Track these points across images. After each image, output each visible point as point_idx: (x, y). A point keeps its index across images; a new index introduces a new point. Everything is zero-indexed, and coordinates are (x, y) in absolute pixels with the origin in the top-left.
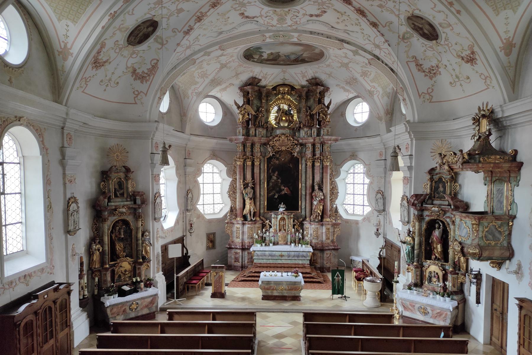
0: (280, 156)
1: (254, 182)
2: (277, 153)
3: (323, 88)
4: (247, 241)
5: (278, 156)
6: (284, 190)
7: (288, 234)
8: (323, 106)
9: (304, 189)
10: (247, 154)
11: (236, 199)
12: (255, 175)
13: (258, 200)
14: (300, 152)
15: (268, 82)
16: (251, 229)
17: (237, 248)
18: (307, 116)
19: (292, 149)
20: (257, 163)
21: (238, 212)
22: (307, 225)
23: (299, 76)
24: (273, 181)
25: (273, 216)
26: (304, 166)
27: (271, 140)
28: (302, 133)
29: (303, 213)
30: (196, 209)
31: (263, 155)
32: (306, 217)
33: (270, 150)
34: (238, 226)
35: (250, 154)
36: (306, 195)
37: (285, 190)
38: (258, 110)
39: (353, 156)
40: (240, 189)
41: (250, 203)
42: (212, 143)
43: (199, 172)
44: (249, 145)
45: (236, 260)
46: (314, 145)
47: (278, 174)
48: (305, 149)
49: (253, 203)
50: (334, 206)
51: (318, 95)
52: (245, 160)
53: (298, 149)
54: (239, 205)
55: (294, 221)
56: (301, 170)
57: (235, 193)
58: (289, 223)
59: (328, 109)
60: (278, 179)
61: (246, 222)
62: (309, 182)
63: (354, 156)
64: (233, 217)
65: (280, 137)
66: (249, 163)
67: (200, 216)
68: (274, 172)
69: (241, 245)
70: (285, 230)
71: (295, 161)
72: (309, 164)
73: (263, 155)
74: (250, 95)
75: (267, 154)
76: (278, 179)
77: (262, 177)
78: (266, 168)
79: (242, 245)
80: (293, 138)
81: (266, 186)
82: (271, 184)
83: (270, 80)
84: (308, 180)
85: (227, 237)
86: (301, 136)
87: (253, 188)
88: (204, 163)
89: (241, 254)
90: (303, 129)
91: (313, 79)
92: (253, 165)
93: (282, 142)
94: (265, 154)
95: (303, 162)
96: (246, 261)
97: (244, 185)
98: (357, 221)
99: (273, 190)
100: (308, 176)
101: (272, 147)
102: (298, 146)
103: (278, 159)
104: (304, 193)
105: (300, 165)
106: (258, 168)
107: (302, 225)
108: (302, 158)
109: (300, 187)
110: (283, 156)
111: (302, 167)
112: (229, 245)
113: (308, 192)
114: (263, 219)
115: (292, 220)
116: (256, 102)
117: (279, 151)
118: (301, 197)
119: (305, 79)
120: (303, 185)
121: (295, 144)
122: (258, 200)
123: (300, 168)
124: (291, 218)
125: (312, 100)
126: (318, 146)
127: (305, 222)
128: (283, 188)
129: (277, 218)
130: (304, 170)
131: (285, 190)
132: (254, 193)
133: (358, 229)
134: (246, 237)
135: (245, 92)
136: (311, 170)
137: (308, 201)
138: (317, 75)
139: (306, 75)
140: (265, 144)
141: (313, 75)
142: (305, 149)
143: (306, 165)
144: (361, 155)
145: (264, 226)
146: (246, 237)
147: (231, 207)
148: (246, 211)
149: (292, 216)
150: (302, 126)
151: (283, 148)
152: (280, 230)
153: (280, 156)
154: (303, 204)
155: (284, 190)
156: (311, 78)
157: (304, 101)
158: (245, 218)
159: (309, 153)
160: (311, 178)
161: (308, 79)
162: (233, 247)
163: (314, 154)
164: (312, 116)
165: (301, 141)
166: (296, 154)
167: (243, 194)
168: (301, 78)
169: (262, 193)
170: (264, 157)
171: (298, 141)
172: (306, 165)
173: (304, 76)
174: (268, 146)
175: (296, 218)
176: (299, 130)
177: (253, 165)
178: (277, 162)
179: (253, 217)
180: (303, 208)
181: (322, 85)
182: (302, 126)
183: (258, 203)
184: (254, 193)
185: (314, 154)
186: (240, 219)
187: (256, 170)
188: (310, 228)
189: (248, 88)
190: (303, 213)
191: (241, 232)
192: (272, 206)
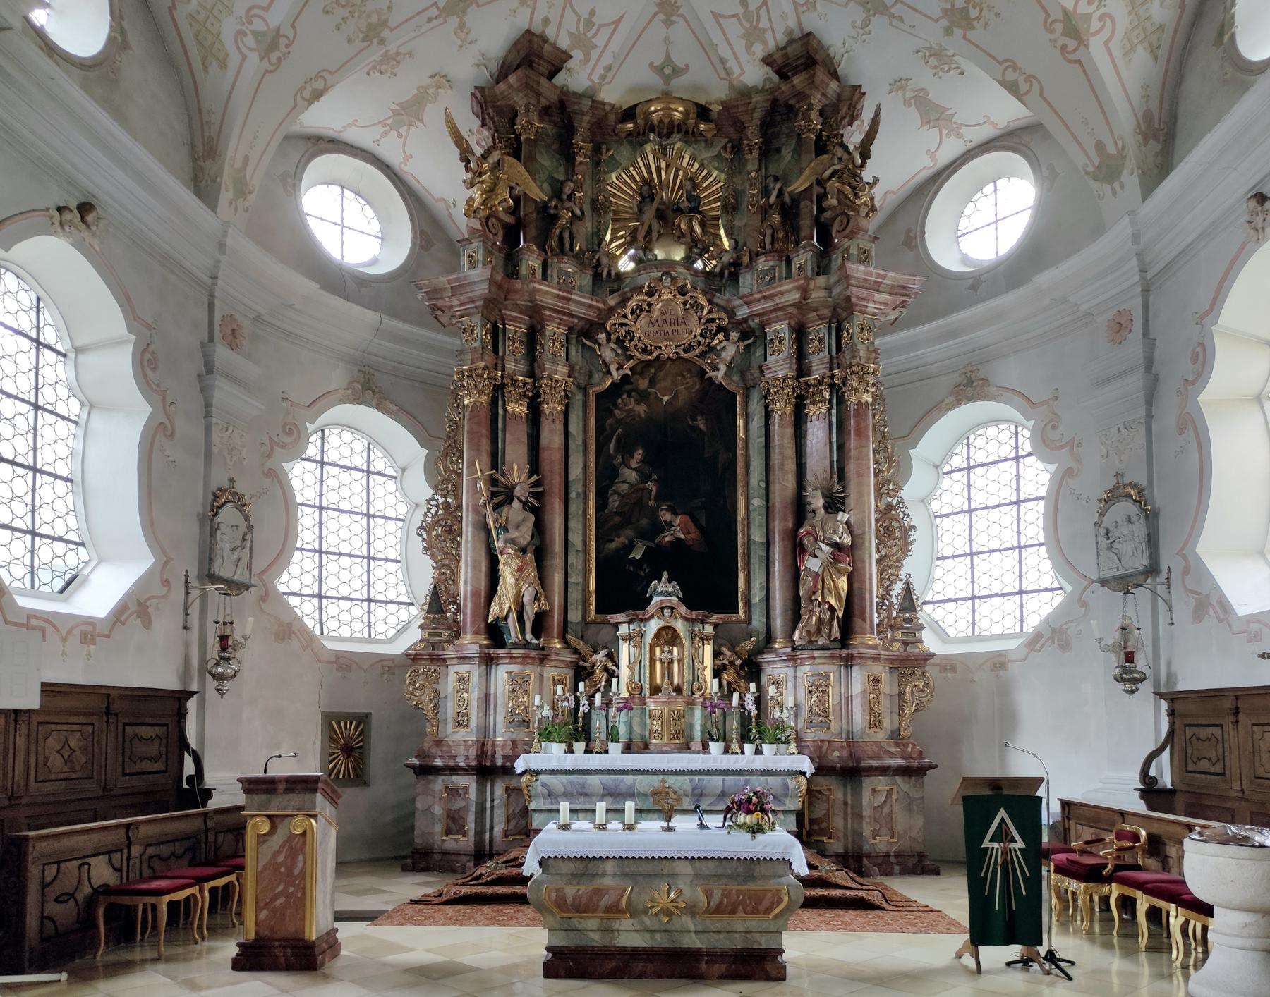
0: (652, 383)
1: (538, 484)
2: (642, 374)
3: (834, 85)
4: (502, 735)
5: (643, 384)
6: (670, 524)
7: (690, 704)
8: (839, 152)
9: (758, 519)
10: (510, 366)
11: (457, 559)
12: (545, 456)
13: (558, 562)
14: (740, 368)
15: (600, 71)
16: (519, 686)
17: (455, 770)
18: (765, 211)
19: (703, 355)
20: (552, 407)
21: (467, 616)
22: (776, 668)
23: (735, 30)
24: (625, 487)
25: (623, 630)
26: (757, 423)
27: (611, 311)
28: (747, 281)
29: (758, 622)
30: (269, 596)
31: (582, 380)
32: (769, 638)
33: (608, 355)
34: (464, 669)
35: (522, 367)
36: (768, 545)
37: (677, 528)
38: (557, 193)
39: (970, 383)
40: (476, 510)
41: (520, 569)
42: (359, 323)
43: (289, 438)
44: (516, 328)
45: (454, 823)
46: (800, 333)
47: (643, 461)
48: (760, 352)
49: (531, 572)
50: (898, 588)
51: (815, 119)
52: (498, 393)
53: (730, 351)
54: (468, 579)
55: (717, 654)
56: (746, 441)
57: (452, 532)
58: (702, 660)
59: (863, 164)
60: (645, 478)
61: (501, 651)
62: (784, 485)
63: (970, 385)
64: (445, 634)
65: (651, 293)
66: (518, 408)
67: (288, 630)
68: (626, 450)
69: (473, 752)
70: (678, 690)
71: (718, 405)
72: (782, 408)
73: (582, 380)
74: (521, 121)
75: (597, 377)
76: (645, 478)
77: (575, 472)
78: (592, 433)
79: (482, 755)
80: (710, 302)
81: (592, 510)
82: (614, 502)
83: (607, 60)
84: (776, 475)
85: (416, 718)
86: (744, 290)
87: (537, 510)
88: (318, 404)
89: (472, 794)
90: (750, 266)
91: (791, 42)
92: (535, 416)
93: (665, 323)
94: (590, 375)
95: (756, 406)
96: (498, 830)
97: (494, 495)
98: (1000, 654)
99: (625, 524)
100: (776, 458)
101: (619, 342)
102: (734, 335)
103: (643, 396)
104: (758, 536)
105: (740, 422)
106: (559, 426)
107: (752, 670)
108: (747, 390)
109: (741, 513)
110: (668, 383)
111: (748, 428)
112: (422, 754)
113: (777, 526)
114: (581, 645)
115: (708, 650)
116: (547, 161)
117: (648, 364)
118: (748, 554)
119: (759, 51)
120: (757, 502)
121: (720, 329)
122: (558, 562)
123: (741, 435)
124: (704, 639)
125: (787, 154)
126: (818, 330)
127: (768, 657)
128: (668, 516)
129: (641, 635)
130: (757, 441)
131: (677, 528)
132: (540, 528)
133: (1004, 692)
134: (500, 719)
135: (499, 111)
136: (790, 431)
137: (777, 568)
138: (812, 22)
139: (764, 24)
140: (584, 332)
141: (792, 23)
142: (760, 352)
143: (768, 414)
144: (1009, 372)
145: (581, 672)
146: (499, 717)
147: (435, 592)
148: (502, 605)
149: (709, 630)
150: (746, 260)
151: (668, 350)
152: (655, 690)
153: (652, 383)
154: (760, 585)
155: (670, 524)
156: (782, 39)
157: (756, 154)
158: (495, 634)
159: (779, 365)
160: (791, 466)
161: (772, 45)
162: (438, 762)
163: (802, 370)
164: (790, 211)
165: (742, 313)
166: (719, 375)
167: (488, 532)
168: (740, 45)
169: (576, 539)
170: (584, 389)
171: (731, 313)
172: (768, 414)
173: (752, 35)
174: (602, 336)
175: (723, 640)
176: (734, 277)
177: (535, 416)
178: (641, 409)
179: (536, 634)
180: (755, 600)
181: (835, 75)
182: (746, 260)
183: (557, 579)
184: (540, 528)
185: (802, 370)
186: (471, 642)
187: (551, 436)
188: (789, 684)
189: (513, 91)
190: (758, 622)
191: (482, 699)
192: (621, 592)
